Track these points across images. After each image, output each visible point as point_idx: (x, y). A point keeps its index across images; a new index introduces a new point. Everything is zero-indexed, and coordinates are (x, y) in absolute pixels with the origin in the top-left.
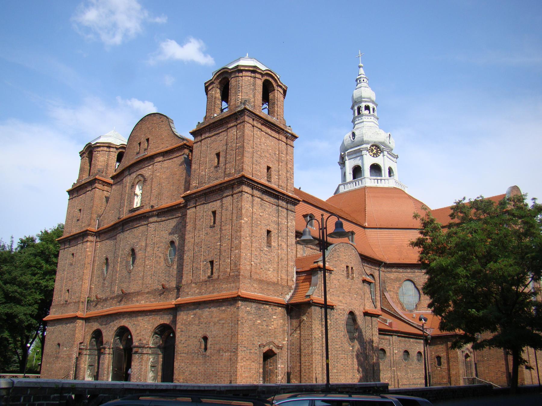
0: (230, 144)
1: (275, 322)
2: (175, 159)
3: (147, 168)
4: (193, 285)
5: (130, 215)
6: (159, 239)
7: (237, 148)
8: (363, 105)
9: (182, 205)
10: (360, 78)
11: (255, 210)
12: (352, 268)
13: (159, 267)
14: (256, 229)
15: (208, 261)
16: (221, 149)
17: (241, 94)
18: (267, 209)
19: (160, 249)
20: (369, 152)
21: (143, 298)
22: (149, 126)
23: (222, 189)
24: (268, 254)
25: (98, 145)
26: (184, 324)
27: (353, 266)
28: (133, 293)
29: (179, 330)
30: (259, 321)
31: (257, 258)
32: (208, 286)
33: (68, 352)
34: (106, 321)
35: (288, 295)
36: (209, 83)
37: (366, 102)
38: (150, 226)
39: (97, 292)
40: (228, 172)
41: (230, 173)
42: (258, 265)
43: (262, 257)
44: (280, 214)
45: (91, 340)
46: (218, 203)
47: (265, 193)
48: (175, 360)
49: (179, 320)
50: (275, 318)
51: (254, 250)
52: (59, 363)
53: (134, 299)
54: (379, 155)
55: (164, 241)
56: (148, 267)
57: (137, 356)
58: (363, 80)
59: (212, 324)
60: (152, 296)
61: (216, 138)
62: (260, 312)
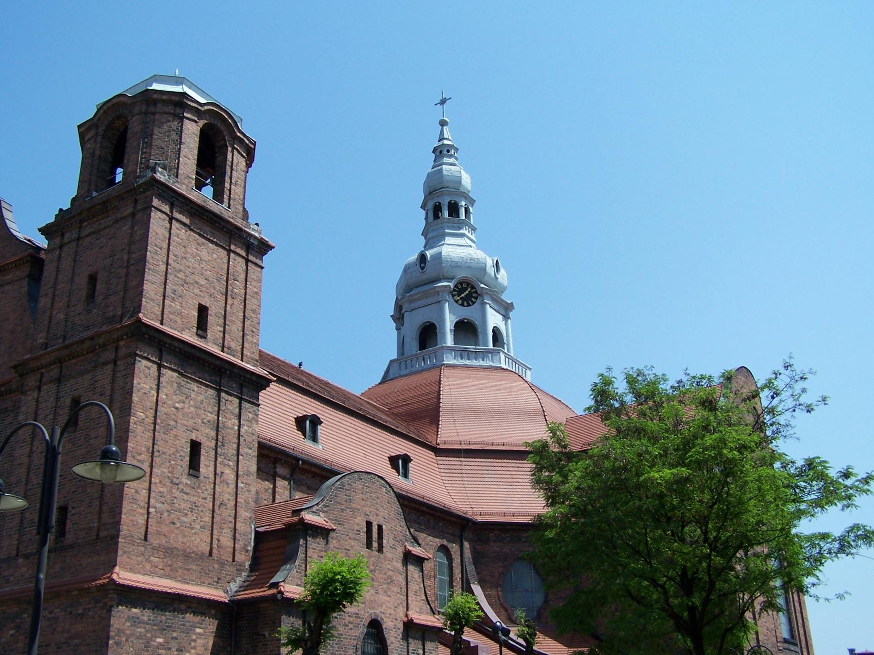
1: (199, 641)
4: (20, 560)
7: (132, 262)
8: (445, 201)
11: (164, 397)
12: (380, 528)
14: (164, 436)
18: (193, 396)
20: (453, 296)
23: (95, 349)
24: (192, 492)
27: (381, 522)
30: (160, 640)
31: (163, 499)
35: (235, 582)
36: (87, 125)
37: (450, 194)
40: (111, 314)
41: (114, 316)
42: (166, 514)
43: (175, 498)
44: (223, 408)
47: (191, 361)
50: (199, 634)
51: (157, 481)
54: (474, 303)
62: (163, 618)
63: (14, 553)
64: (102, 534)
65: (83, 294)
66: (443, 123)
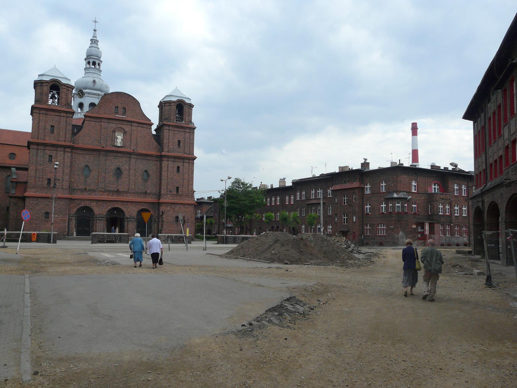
2: (145, 129)
3: (126, 126)
4: (168, 195)
10: (97, 40)
19: (137, 172)
25: (69, 86)
28: (121, 191)
32: (177, 197)
34: (96, 203)
39: (78, 185)
46: (181, 164)
53: (124, 195)
63: (166, 193)
64: (189, 194)
65: (177, 144)
66: (95, 31)
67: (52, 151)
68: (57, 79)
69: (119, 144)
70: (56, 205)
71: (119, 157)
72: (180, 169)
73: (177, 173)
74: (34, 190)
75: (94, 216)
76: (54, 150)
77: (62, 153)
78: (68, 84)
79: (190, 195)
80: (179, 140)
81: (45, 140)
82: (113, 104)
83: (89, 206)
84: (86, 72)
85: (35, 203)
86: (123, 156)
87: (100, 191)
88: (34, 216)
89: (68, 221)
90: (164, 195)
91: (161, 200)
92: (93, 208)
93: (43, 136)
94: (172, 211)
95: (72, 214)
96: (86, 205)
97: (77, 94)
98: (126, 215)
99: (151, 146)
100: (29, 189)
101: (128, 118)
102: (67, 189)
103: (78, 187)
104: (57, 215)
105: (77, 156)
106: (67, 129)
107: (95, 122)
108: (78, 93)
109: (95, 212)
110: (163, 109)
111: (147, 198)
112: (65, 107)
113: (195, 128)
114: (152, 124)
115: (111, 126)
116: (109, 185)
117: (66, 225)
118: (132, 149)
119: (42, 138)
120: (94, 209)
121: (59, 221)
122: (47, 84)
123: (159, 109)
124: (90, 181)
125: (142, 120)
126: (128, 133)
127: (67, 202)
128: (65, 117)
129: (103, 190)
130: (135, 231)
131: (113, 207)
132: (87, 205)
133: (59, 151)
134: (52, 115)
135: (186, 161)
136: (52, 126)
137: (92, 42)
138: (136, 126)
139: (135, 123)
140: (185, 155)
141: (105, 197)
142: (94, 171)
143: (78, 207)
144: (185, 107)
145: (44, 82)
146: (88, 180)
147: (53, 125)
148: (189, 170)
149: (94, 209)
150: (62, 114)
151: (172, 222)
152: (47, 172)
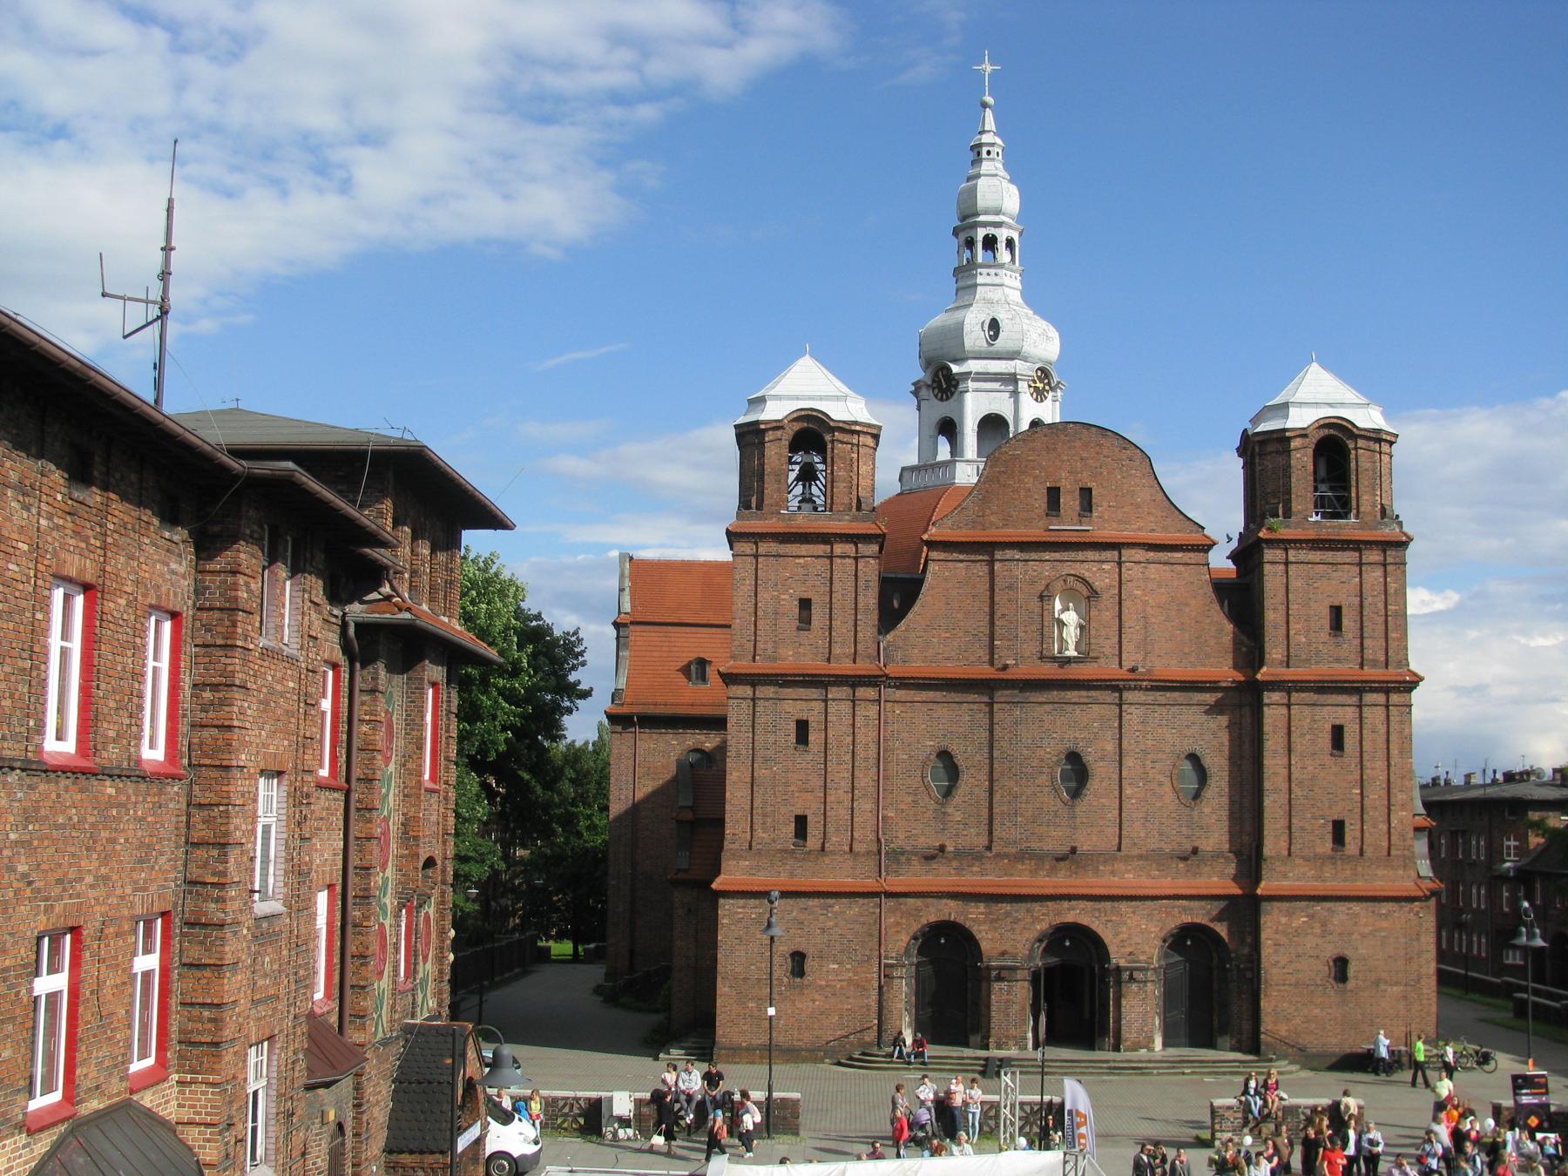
0: (1370, 599)
4: (1298, 861)
5: (1049, 671)
6: (1155, 743)
9: (1224, 685)
10: (993, 145)
13: (1159, 804)
15: (1331, 819)
16: (1348, 602)
17: (1379, 493)
20: (1030, 386)
21: (1129, 867)
22: (1085, 455)
25: (858, 428)
26: (1284, 932)
29: (1269, 942)
32: (1339, 867)
33: (851, 974)
36: (1298, 433)
37: (1010, 227)
38: (1129, 711)
45: (908, 944)
48: (1262, 996)
49: (1269, 924)
52: (814, 1001)
53: (1101, 868)
54: (1046, 398)
55: (1167, 751)
56: (1134, 801)
57: (1134, 987)
58: (998, 153)
59: (1355, 936)
60: (1154, 865)
61: (1329, 571)
64: (1393, 852)
65: (1326, 622)
67: (806, 700)
68: (812, 410)
69: (1072, 646)
70: (831, 923)
71: (1075, 703)
72: (1346, 735)
73: (1332, 755)
74: (747, 863)
75: (982, 961)
76: (815, 696)
77: (845, 707)
78: (856, 423)
79: (1399, 853)
80: (1336, 604)
81: (775, 659)
82: (1036, 477)
83: (960, 920)
84: (961, 284)
85: (753, 916)
86: (1088, 697)
87: (999, 856)
88: (752, 967)
89: (876, 985)
90: (1277, 864)
91: (1263, 884)
92: (975, 929)
93: (770, 646)
94: (1317, 931)
95: (894, 955)
96: (947, 918)
97: (929, 383)
98: (1112, 956)
99: (1212, 642)
100: (730, 863)
101: (1105, 528)
102: (868, 853)
103: (914, 843)
104: (835, 962)
105: (904, 715)
106: (860, 606)
107: (970, 564)
108: (934, 381)
109: (984, 946)
110: (1258, 468)
111: (1201, 874)
112: (847, 517)
113: (1402, 544)
114: (1206, 547)
115: (1036, 573)
116: (1036, 831)
117: (873, 1004)
118: (1127, 665)
119: (769, 652)
120: (980, 931)
121: (842, 988)
122: (779, 433)
123: (1241, 461)
124: (958, 816)
125: (1165, 529)
126: (1105, 596)
127: (871, 910)
128: (849, 557)
129: (1014, 850)
130: (1154, 1024)
131: (1058, 920)
132: (950, 914)
133: (834, 700)
134: (799, 557)
135: (1369, 698)
136: (805, 604)
137: (979, 154)
138: (1140, 562)
139: (1133, 551)
140: (1370, 673)
141: (1022, 879)
142: (972, 770)
143: (915, 927)
144: (1353, 452)
145: (768, 426)
146: (950, 810)
147: (805, 596)
148: (1388, 741)
149: (980, 931)
150: (839, 548)
151: (1319, 982)
152: (790, 789)
